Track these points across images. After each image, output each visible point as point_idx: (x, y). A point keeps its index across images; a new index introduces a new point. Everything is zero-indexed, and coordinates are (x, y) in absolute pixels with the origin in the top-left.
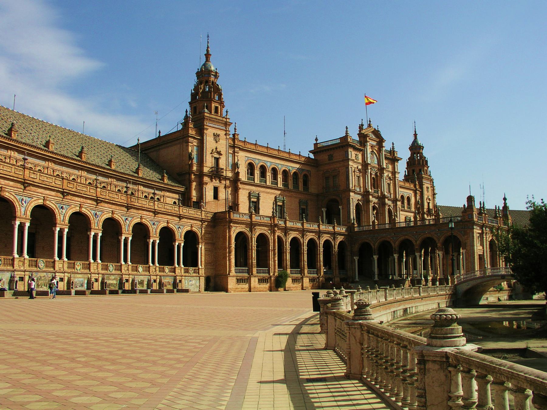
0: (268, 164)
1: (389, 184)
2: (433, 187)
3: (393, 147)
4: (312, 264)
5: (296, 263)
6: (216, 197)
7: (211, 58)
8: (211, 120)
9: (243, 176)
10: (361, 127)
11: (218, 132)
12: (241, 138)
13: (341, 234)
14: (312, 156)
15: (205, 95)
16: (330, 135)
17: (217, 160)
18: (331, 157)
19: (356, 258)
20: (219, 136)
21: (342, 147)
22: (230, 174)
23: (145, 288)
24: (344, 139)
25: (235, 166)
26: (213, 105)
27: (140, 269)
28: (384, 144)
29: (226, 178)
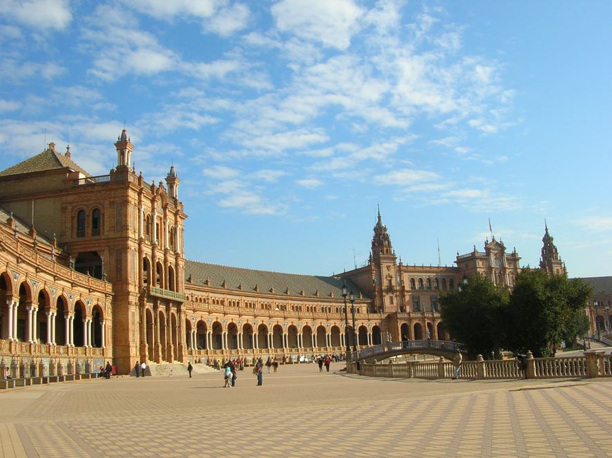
0: (424, 277)
3: (515, 251)
6: (392, 303)
8: (385, 258)
9: (407, 288)
10: (486, 244)
11: (390, 264)
12: (404, 264)
14: (455, 265)
15: (381, 240)
16: (466, 251)
17: (390, 281)
18: (467, 266)
21: (473, 259)
22: (398, 288)
24: (473, 254)
25: (402, 281)
26: (385, 249)
28: (505, 251)
29: (396, 291)
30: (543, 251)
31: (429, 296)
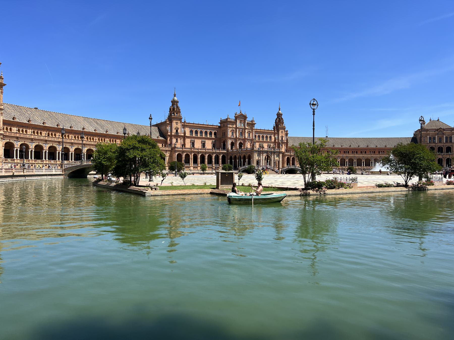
1: (249, 134)
2: (287, 131)
9: (188, 134)
14: (219, 125)
17: (177, 131)
22: (183, 135)
24: (227, 119)
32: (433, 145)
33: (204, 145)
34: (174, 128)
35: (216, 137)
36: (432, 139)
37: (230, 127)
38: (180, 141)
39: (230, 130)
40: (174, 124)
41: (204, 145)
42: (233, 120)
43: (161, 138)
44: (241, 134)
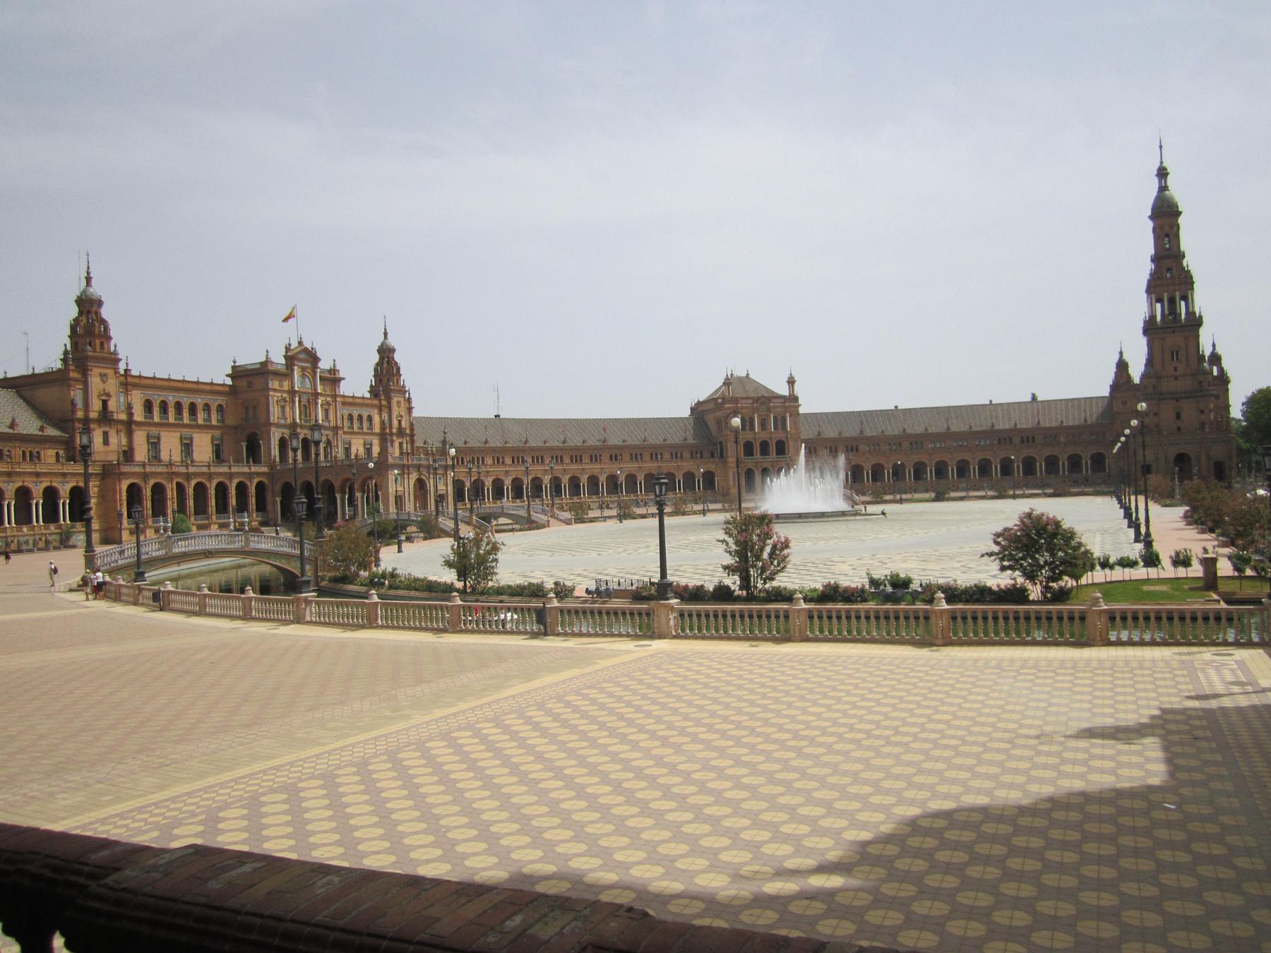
1: (327, 411)
2: (409, 401)
4: (222, 508)
5: (201, 509)
7: (93, 282)
9: (139, 415)
10: (288, 349)
13: (258, 474)
14: (229, 381)
15: (89, 327)
16: (251, 358)
17: (105, 403)
18: (250, 384)
19: (278, 499)
20: (106, 375)
21: (262, 373)
22: (123, 417)
23: (31, 547)
24: (264, 364)
25: (129, 407)
26: (98, 342)
27: (25, 530)
30: (376, 370)
31: (178, 435)
32: (748, 436)
33: (187, 447)
34: (95, 396)
35: (223, 421)
36: (747, 423)
37: (275, 390)
38: (118, 440)
39: (274, 397)
40: (95, 381)
41: (187, 447)
42: (283, 369)
43: (51, 432)
44: (306, 409)
